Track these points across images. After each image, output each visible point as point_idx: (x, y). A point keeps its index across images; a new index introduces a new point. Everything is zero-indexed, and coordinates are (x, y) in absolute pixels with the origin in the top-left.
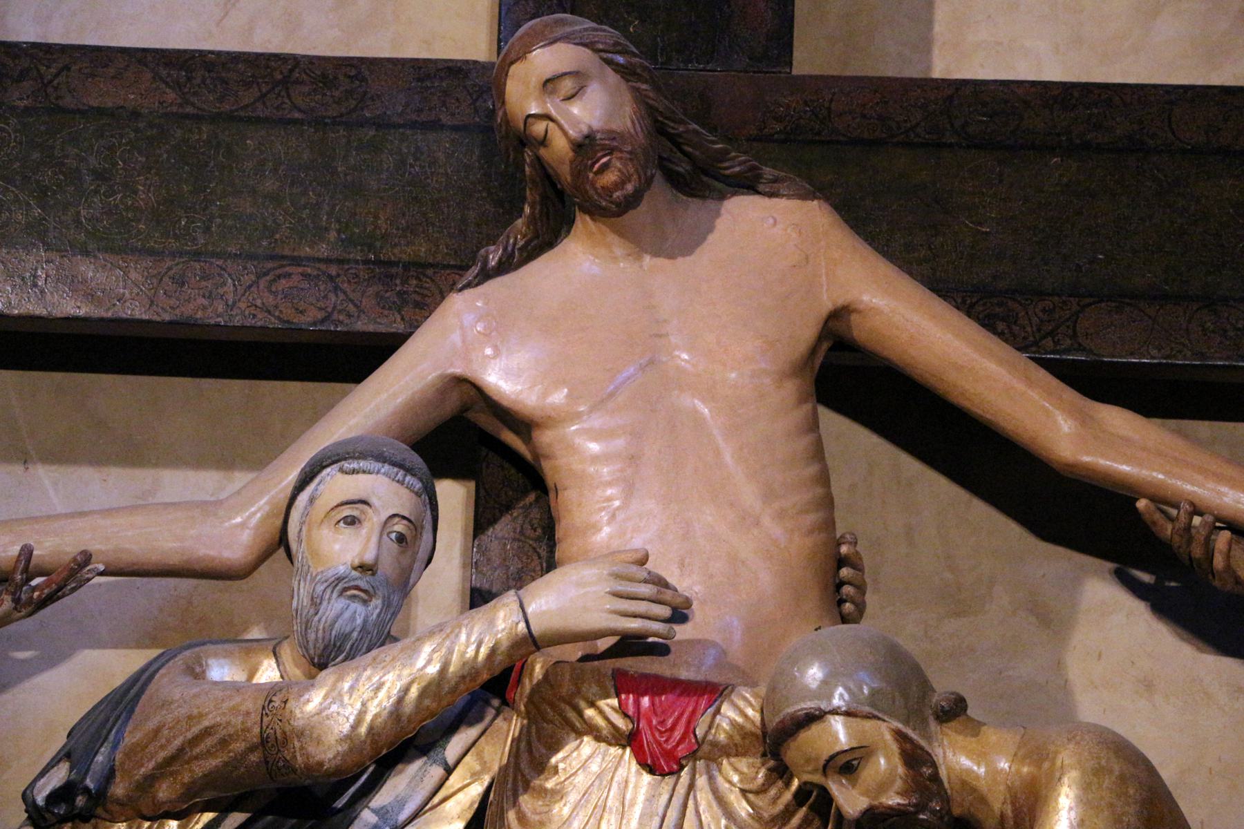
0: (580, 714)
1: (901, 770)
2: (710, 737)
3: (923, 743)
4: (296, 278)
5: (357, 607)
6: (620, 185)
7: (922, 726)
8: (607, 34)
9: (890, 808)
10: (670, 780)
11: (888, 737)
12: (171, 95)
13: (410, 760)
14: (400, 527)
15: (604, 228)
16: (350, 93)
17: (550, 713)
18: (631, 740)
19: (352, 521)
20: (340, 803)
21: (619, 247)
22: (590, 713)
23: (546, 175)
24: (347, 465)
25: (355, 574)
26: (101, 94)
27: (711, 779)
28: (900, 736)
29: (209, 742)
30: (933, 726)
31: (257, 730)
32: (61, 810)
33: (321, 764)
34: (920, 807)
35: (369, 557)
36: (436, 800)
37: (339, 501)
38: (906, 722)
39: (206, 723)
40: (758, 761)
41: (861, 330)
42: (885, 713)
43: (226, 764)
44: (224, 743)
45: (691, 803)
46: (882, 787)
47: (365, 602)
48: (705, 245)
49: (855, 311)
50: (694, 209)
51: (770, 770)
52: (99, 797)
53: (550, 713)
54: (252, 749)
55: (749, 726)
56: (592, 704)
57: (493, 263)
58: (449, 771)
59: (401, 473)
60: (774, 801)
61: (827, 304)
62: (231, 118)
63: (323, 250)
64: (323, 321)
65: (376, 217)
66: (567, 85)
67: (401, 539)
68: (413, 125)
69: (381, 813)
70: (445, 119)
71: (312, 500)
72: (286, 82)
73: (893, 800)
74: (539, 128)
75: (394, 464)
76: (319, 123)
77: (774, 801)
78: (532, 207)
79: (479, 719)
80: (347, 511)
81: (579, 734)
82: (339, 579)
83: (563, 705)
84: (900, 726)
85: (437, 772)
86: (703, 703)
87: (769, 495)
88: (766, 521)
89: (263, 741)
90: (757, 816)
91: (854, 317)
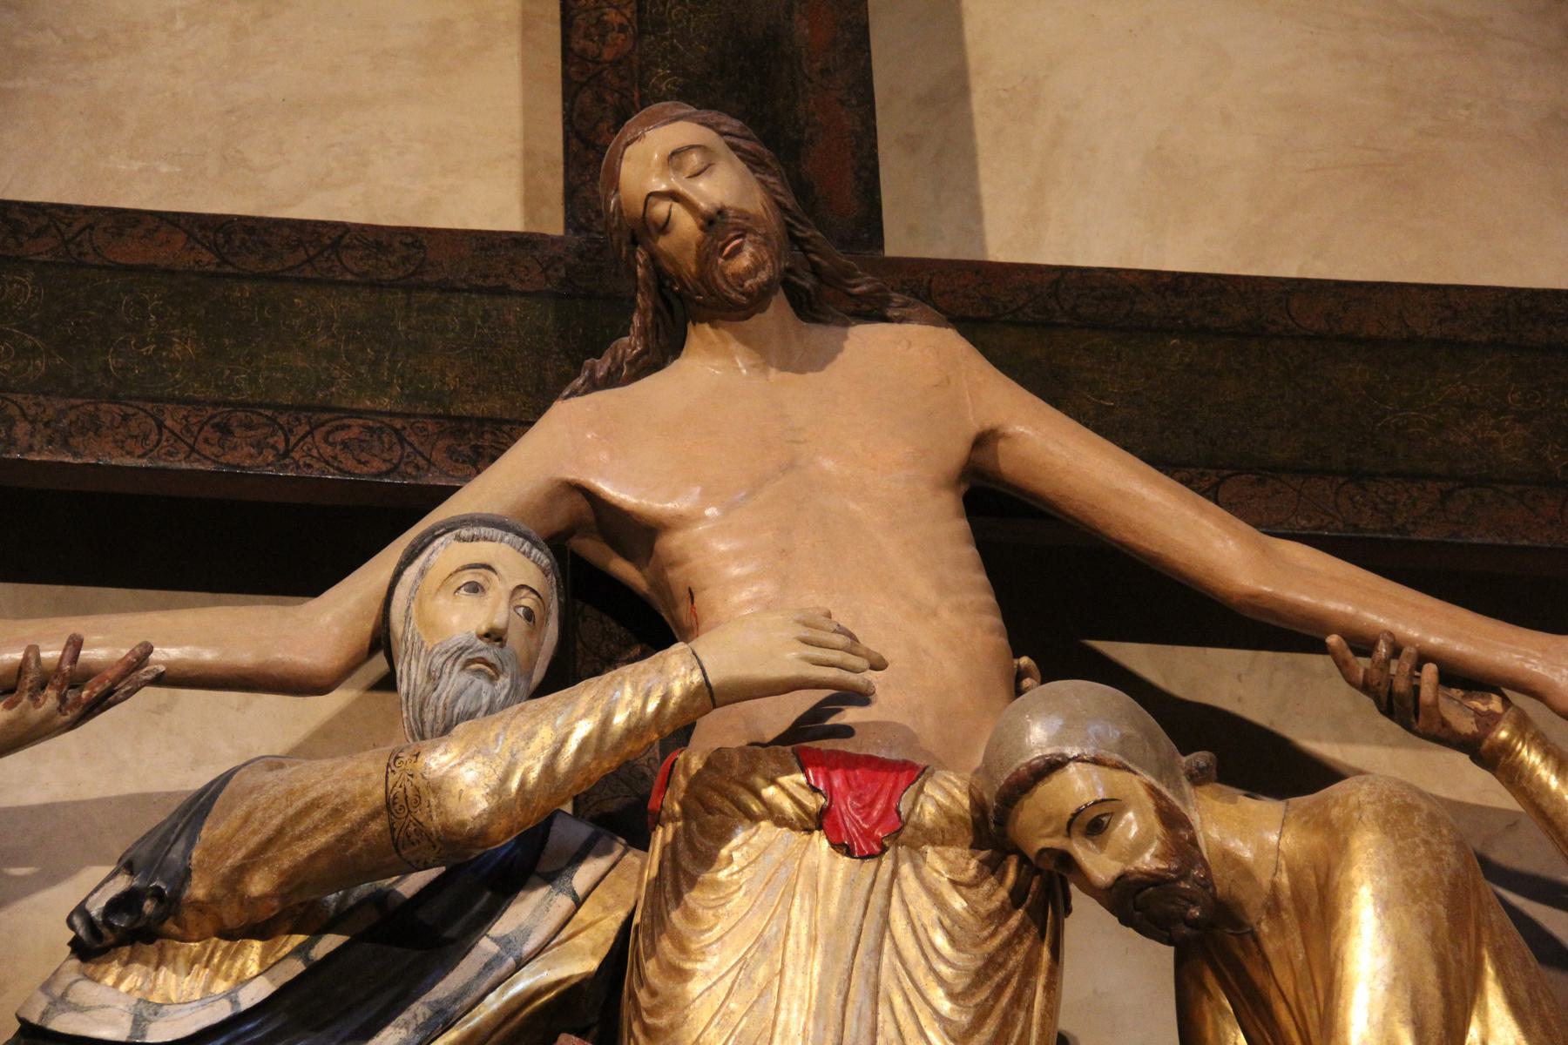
0: (758, 795)
1: (1158, 829)
2: (914, 819)
3: (1178, 803)
4: (356, 430)
5: (481, 682)
6: (752, 272)
7: (1177, 787)
8: (734, 124)
9: (1148, 873)
10: (871, 865)
11: (1142, 793)
12: (206, 256)
13: (534, 888)
14: (528, 601)
15: (726, 334)
16: (406, 259)
17: (717, 800)
18: (821, 821)
19: (475, 588)
20: (451, 932)
21: (742, 362)
22: (770, 792)
23: (663, 277)
24: (464, 532)
25: (481, 644)
26: (129, 251)
27: (916, 868)
28: (1152, 790)
29: (317, 815)
30: (1187, 787)
31: (381, 791)
32: (121, 922)
33: (462, 824)
34: (1183, 874)
35: (499, 620)
36: (563, 935)
37: (459, 565)
38: (1159, 778)
39: (313, 794)
40: (967, 852)
41: (1009, 462)
42: (1138, 764)
43: (339, 839)
44: (337, 813)
45: (895, 891)
46: (1138, 848)
47: (492, 679)
48: (835, 363)
49: (1004, 436)
50: (818, 334)
51: (982, 862)
52: (170, 903)
53: (717, 800)
54: (373, 816)
55: (956, 810)
56: (773, 782)
57: (600, 374)
58: (578, 903)
59: (527, 546)
60: (989, 897)
61: (973, 426)
62: (275, 278)
63: (385, 403)
64: (388, 473)
65: (444, 375)
66: (694, 160)
67: (529, 615)
68: (479, 290)
69: (504, 942)
70: (514, 285)
71: (422, 573)
72: (336, 245)
74: (661, 209)
75: (519, 534)
76: (377, 286)
77: (989, 897)
78: (643, 314)
79: (608, 851)
80: (468, 577)
81: (754, 819)
82: (463, 649)
83: (734, 787)
84: (1153, 781)
85: (564, 903)
86: (903, 783)
87: (942, 588)
88: (945, 613)
89: (389, 803)
90: (972, 908)
91: (1002, 444)
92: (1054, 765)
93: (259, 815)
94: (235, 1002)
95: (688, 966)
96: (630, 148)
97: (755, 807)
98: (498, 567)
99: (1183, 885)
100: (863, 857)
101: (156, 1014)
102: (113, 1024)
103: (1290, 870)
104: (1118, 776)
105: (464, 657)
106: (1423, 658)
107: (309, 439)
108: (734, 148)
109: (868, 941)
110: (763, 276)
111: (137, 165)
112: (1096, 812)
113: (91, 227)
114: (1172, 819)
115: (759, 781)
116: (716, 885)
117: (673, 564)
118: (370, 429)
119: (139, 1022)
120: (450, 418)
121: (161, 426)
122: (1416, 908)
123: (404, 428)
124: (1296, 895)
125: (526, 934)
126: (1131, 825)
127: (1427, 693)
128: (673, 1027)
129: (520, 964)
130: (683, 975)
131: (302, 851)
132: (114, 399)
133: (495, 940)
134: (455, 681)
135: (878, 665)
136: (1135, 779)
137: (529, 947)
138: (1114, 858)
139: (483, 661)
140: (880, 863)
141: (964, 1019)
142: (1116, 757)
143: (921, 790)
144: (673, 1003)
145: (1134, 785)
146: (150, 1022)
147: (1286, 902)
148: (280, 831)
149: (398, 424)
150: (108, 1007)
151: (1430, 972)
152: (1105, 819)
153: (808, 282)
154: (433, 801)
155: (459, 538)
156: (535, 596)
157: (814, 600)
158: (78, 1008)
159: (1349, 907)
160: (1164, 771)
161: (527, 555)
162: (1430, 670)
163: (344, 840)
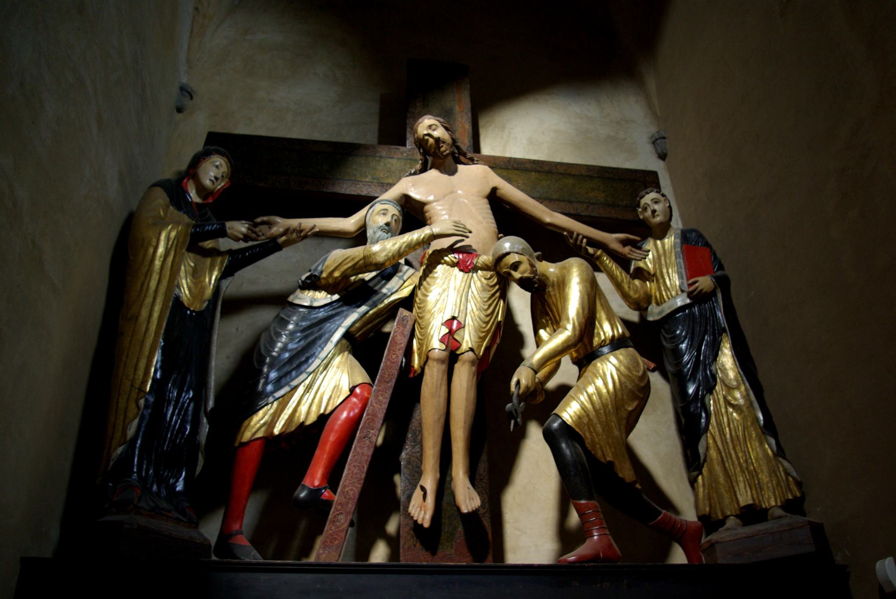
5: (385, 234)
6: (445, 151)
19: (384, 214)
29: (349, 260)
30: (536, 260)
33: (380, 262)
36: (402, 287)
41: (499, 193)
44: (353, 259)
46: (524, 272)
47: (387, 233)
58: (405, 282)
59: (395, 206)
66: (434, 127)
69: (389, 290)
70: (395, 157)
71: (373, 211)
74: (426, 137)
77: (492, 281)
80: (382, 212)
82: (381, 227)
87: (484, 218)
88: (484, 223)
91: (498, 190)
92: (508, 254)
93: (337, 260)
94: (331, 299)
95: (427, 294)
96: (420, 125)
98: (389, 210)
99: (534, 280)
100: (466, 273)
102: (306, 302)
103: (557, 277)
104: (522, 256)
105: (381, 228)
106: (584, 237)
108: (442, 125)
109: (466, 290)
110: (448, 152)
114: (532, 266)
116: (434, 278)
117: (427, 212)
119: (311, 302)
120: (381, 183)
122: (584, 284)
124: (558, 282)
125: (393, 288)
126: (524, 267)
127: (584, 245)
128: (424, 307)
129: (392, 294)
131: (346, 267)
133: (387, 289)
134: (379, 233)
135: (470, 232)
136: (525, 257)
137: (394, 290)
138: (520, 273)
139: (385, 229)
140: (469, 275)
141: (486, 307)
142: (521, 252)
143: (478, 258)
144: (423, 301)
145: (524, 259)
147: (555, 284)
148: (341, 263)
149: (370, 184)
151: (586, 297)
155: (381, 204)
157: (456, 219)
158: (300, 299)
159: (570, 284)
160: (531, 255)
161: (395, 208)
162: (585, 240)
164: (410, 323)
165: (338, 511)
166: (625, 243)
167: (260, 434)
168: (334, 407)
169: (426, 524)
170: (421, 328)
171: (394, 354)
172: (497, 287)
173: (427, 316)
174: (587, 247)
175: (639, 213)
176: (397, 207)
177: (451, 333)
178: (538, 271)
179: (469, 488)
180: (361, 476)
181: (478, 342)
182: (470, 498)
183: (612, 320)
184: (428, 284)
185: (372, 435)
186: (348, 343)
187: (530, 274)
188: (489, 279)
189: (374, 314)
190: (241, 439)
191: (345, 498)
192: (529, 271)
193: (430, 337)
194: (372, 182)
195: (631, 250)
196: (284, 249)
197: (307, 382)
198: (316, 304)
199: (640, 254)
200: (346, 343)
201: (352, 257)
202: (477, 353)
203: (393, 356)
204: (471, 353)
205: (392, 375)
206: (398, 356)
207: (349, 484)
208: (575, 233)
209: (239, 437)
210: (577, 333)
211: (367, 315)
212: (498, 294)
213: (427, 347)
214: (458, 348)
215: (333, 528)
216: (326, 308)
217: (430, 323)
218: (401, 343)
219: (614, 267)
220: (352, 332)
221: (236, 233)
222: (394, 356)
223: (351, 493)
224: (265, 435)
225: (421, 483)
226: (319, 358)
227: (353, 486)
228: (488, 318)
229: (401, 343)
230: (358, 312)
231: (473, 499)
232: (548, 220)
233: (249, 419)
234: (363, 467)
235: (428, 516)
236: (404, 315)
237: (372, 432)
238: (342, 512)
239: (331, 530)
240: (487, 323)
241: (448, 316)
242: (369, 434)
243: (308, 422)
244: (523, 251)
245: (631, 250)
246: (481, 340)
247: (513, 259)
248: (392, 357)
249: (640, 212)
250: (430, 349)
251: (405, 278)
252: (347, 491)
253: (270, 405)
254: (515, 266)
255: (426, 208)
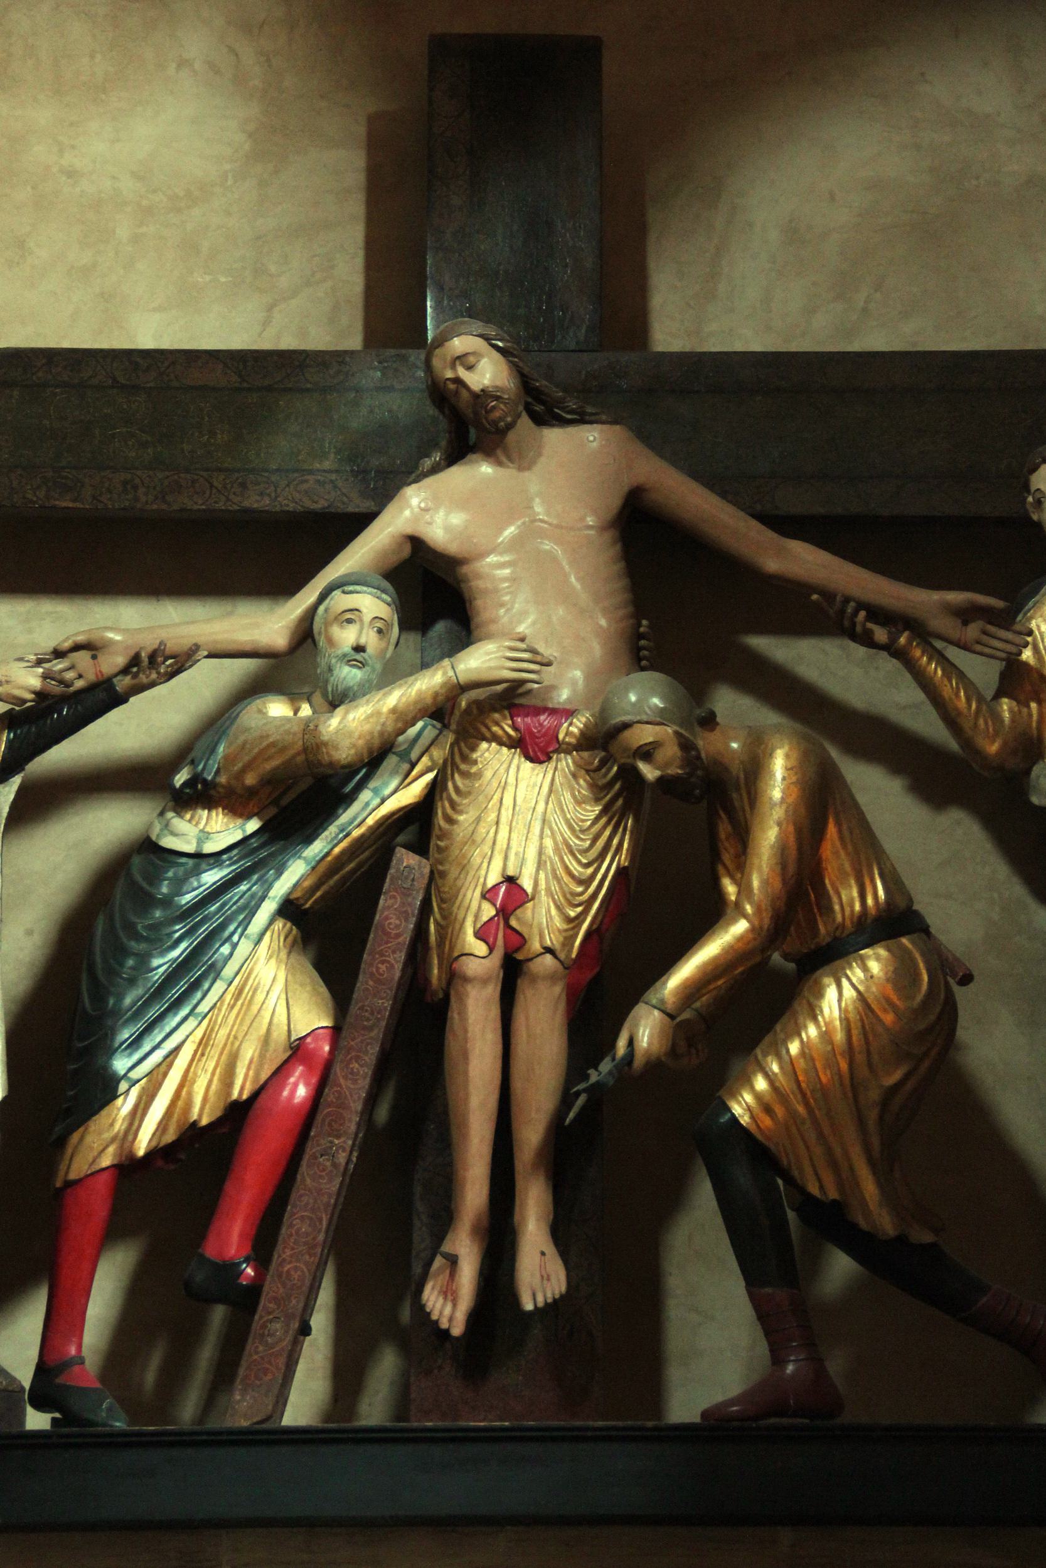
0: (489, 729)
1: (679, 754)
3: (691, 738)
14: (379, 624)
22: (495, 729)
24: (347, 588)
30: (698, 729)
31: (300, 743)
33: (339, 761)
38: (681, 727)
44: (283, 749)
46: (667, 765)
54: (298, 754)
63: (327, 465)
67: (380, 631)
70: (397, 386)
71: (326, 610)
73: (675, 770)
89: (305, 750)
92: (626, 726)
93: (248, 746)
95: (455, 816)
96: (437, 350)
97: (488, 735)
99: (693, 780)
100: (541, 762)
101: (207, 838)
102: (188, 842)
107: (287, 489)
111: (208, 278)
112: (648, 748)
113: (173, 363)
115: (490, 724)
118: (318, 481)
119: (200, 842)
121: (212, 486)
123: (336, 479)
130: (479, 775)
132: (187, 471)
142: (658, 719)
146: (205, 843)
149: (334, 477)
150: (185, 835)
152: (651, 751)
153: (539, 408)
154: (324, 750)
155: (344, 592)
156: (382, 621)
163: (287, 763)
164: (421, 884)
165: (270, 1313)
166: (965, 614)
167: (106, 1161)
168: (257, 1087)
169: (457, 1331)
170: (443, 901)
171: (383, 962)
172: (617, 786)
173: (453, 873)
174: (870, 625)
175: (1028, 506)
176: (384, 596)
177: (505, 913)
178: (703, 755)
179: (543, 1254)
180: (314, 1239)
181: (566, 930)
182: (542, 1277)
183: (865, 872)
184: (457, 790)
185: (337, 1150)
186: (289, 925)
187: (681, 767)
188: (598, 769)
189: (343, 852)
190: (67, 1173)
191: (284, 1285)
192: (678, 762)
193: (457, 926)
194: (337, 471)
195: (985, 633)
196: (132, 699)
197: (199, 1033)
198: (210, 848)
199: (1007, 641)
200: (284, 926)
201: (280, 745)
202: (562, 956)
203: (380, 965)
204: (548, 957)
205: (378, 1013)
206: (392, 966)
207: (291, 1256)
208: (838, 598)
209: (63, 1167)
210: (767, 922)
211: (329, 858)
212: (620, 802)
213: (452, 949)
214: (519, 949)
215: (261, 1348)
216: (235, 852)
217: (459, 891)
218: (398, 936)
219: (939, 672)
220: (297, 899)
221: (18, 693)
222: (383, 967)
223: (296, 1275)
224: (115, 1162)
225: (446, 1247)
226: (222, 979)
227: (298, 1261)
228: (590, 870)
229: (398, 936)
230: (305, 859)
231: (549, 1279)
232: (772, 565)
233: (81, 1129)
234: (320, 1220)
235: (461, 1315)
236: (405, 864)
237: (336, 1142)
238: (277, 1316)
239: (257, 1353)
240: (586, 882)
241: (493, 878)
242: (331, 1148)
243: (205, 1121)
244: (661, 717)
245: (985, 633)
246: (571, 926)
247: (645, 735)
248: (378, 969)
249: (1031, 503)
250: (456, 954)
251: (414, 756)
252: (288, 1271)
253: (122, 1097)
254: (646, 753)
255: (465, 569)
